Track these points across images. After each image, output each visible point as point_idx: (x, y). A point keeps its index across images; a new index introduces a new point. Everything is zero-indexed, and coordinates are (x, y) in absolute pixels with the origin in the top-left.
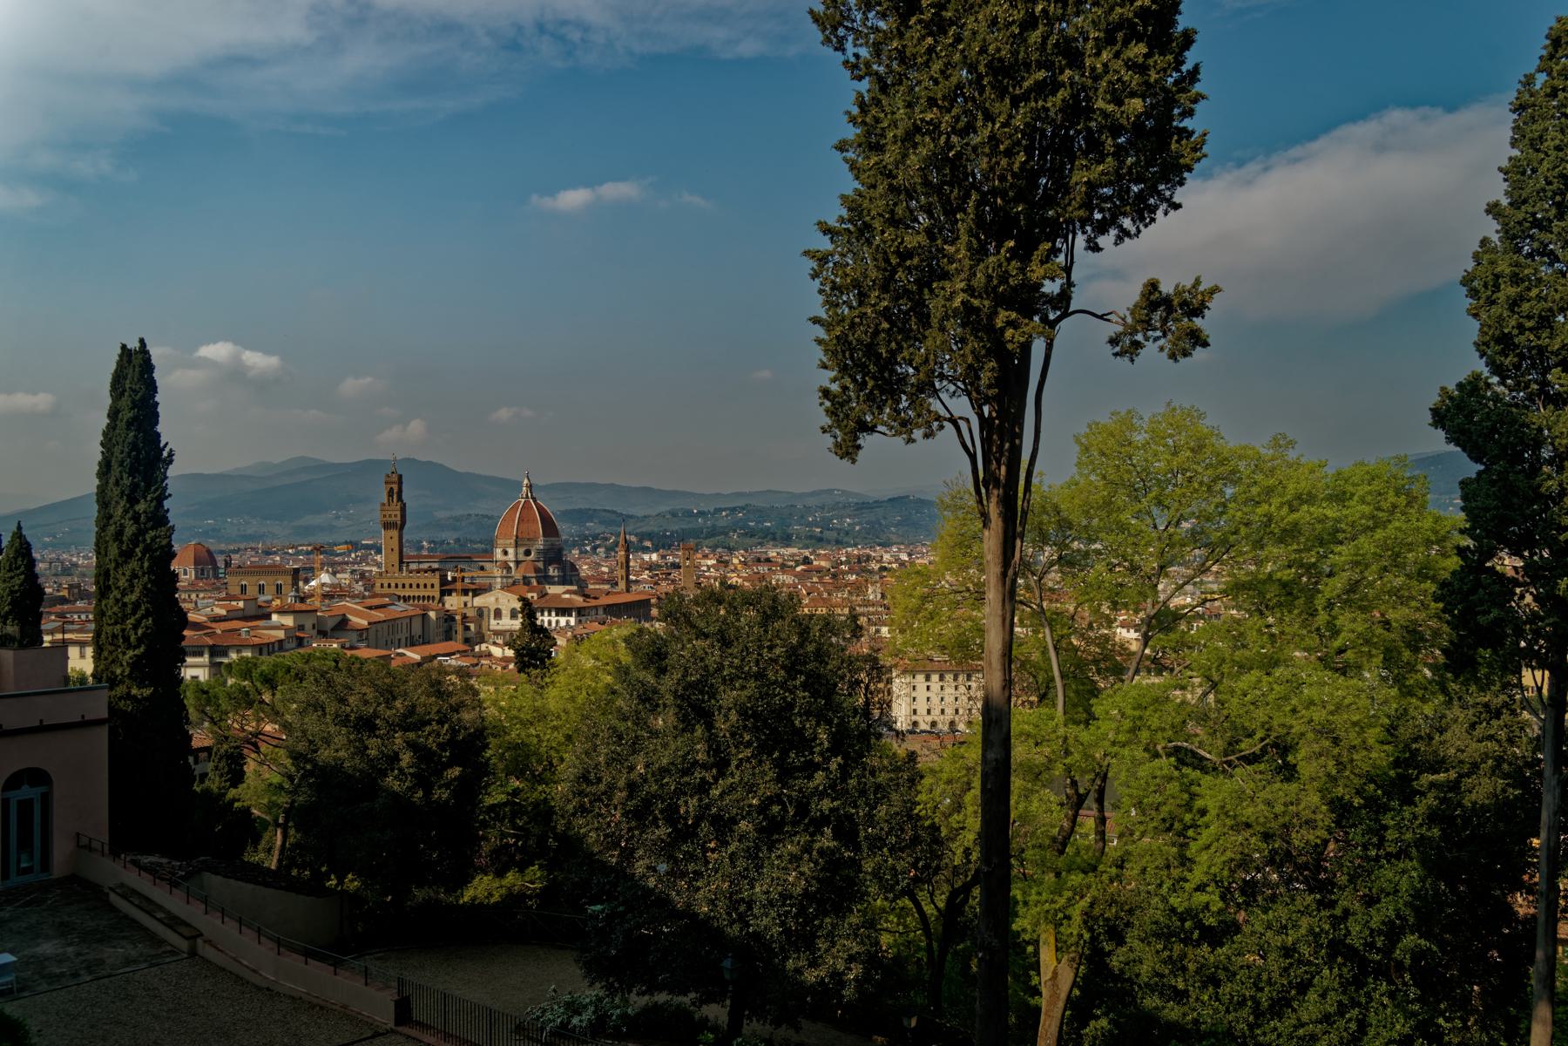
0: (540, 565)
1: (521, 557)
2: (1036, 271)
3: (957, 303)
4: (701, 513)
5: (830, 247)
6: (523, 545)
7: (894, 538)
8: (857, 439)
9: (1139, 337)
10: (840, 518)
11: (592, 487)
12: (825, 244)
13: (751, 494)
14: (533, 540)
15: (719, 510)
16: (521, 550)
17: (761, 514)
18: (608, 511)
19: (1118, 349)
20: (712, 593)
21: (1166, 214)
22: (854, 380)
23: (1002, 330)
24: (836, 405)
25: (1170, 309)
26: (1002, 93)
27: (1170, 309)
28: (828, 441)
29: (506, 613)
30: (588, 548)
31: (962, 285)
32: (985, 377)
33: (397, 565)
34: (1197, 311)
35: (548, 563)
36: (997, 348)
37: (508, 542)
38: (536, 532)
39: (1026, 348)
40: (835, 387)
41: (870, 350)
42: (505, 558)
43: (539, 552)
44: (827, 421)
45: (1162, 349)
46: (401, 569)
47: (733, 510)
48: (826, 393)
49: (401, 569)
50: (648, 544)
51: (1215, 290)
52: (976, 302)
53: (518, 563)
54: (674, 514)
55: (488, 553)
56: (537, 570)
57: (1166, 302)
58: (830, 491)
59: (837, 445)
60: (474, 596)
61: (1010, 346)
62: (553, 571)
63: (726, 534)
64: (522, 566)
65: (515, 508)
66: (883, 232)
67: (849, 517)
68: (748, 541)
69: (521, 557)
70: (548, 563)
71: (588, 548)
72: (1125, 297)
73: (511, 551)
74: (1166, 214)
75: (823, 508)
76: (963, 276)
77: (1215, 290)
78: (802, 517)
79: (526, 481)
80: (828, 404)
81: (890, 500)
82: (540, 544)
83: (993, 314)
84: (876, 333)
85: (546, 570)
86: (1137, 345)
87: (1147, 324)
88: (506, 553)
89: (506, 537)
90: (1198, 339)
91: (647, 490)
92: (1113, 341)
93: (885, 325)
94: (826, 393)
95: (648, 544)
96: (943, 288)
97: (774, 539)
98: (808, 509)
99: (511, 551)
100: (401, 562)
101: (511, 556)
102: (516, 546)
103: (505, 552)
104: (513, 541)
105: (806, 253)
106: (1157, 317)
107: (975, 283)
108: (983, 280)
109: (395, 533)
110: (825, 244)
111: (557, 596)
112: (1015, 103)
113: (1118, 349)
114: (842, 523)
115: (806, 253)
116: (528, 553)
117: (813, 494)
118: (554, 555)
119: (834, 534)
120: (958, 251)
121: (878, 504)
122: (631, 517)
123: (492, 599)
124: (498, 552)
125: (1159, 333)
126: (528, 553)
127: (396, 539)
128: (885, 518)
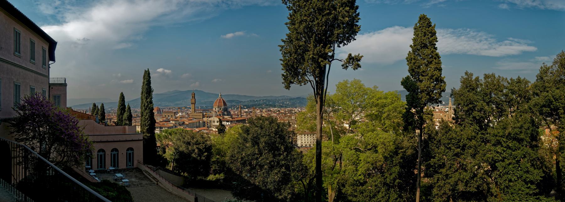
0: (223, 112)
1: (219, 110)
2: (327, 50)
3: (311, 56)
4: (257, 101)
5: (284, 45)
7: (297, 106)
8: (290, 85)
9: (348, 65)
10: (286, 102)
11: (234, 95)
12: (283, 44)
13: (267, 97)
14: (222, 106)
15: (260, 100)
16: (219, 109)
17: (269, 101)
19: (343, 67)
20: (259, 118)
21: (353, 41)
22: (289, 73)
23: (320, 62)
24: (285, 78)
25: (354, 60)
26: (320, 14)
27: (354, 60)
28: (284, 85)
29: (216, 121)
30: (233, 108)
31: (312, 53)
32: (317, 72)
34: (359, 60)
35: (224, 111)
36: (319, 66)
38: (222, 105)
39: (325, 66)
40: (285, 74)
41: (293, 66)
42: (216, 110)
43: (223, 109)
44: (283, 81)
45: (352, 68)
46: (195, 112)
47: (263, 100)
48: (283, 75)
49: (195, 112)
50: (245, 107)
51: (362, 56)
52: (315, 57)
53: (218, 111)
54: (251, 101)
55: (212, 109)
56: (222, 113)
57: (353, 58)
59: (286, 86)
61: (322, 66)
62: (225, 113)
63: (262, 105)
64: (219, 112)
66: (295, 42)
69: (219, 110)
70: (224, 111)
72: (345, 57)
73: (217, 109)
74: (353, 41)
75: (282, 99)
76: (312, 51)
77: (362, 56)
78: (278, 102)
79: (220, 94)
80: (283, 77)
81: (297, 98)
82: (223, 107)
83: (318, 59)
84: (294, 62)
85: (224, 113)
86: (347, 66)
87: (349, 62)
88: (216, 109)
89: (216, 106)
90: (359, 66)
91: (245, 96)
92: (343, 66)
93: (296, 61)
94: (283, 75)
95: (245, 107)
96: (308, 53)
97: (272, 106)
98: (279, 100)
99: (217, 109)
100: (195, 111)
101: (217, 110)
103: (216, 109)
104: (217, 107)
105: (279, 46)
106: (351, 61)
107: (314, 52)
108: (316, 52)
109: (194, 105)
110: (283, 44)
111: (227, 118)
112: (323, 16)
113: (343, 67)
114: (286, 103)
115: (279, 46)
116: (220, 109)
117: (280, 97)
118: (226, 110)
119: (285, 105)
120: (311, 46)
122: (241, 101)
124: (214, 109)
125: (351, 64)
126: (220, 109)
127: (194, 107)
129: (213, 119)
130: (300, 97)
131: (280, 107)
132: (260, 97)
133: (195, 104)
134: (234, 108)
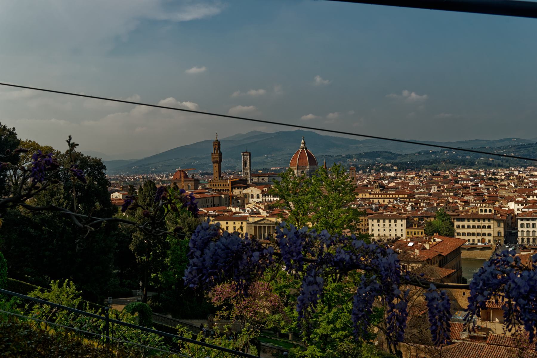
6: (300, 169)
13: (466, 142)
14: (305, 166)
16: (300, 171)
18: (386, 152)
30: (367, 170)
33: (218, 177)
37: (295, 167)
43: (307, 172)
46: (219, 179)
49: (219, 179)
50: (396, 168)
54: (419, 153)
58: (510, 139)
60: (243, 189)
63: (439, 162)
68: (449, 166)
71: (367, 170)
75: (500, 148)
95: (396, 168)
97: (464, 164)
102: (298, 169)
104: (296, 167)
117: (501, 141)
122: (399, 155)
126: (302, 172)
127: (217, 168)
128: (533, 153)
129: (250, 190)
131: (485, 165)
133: (220, 161)
134: (370, 170)
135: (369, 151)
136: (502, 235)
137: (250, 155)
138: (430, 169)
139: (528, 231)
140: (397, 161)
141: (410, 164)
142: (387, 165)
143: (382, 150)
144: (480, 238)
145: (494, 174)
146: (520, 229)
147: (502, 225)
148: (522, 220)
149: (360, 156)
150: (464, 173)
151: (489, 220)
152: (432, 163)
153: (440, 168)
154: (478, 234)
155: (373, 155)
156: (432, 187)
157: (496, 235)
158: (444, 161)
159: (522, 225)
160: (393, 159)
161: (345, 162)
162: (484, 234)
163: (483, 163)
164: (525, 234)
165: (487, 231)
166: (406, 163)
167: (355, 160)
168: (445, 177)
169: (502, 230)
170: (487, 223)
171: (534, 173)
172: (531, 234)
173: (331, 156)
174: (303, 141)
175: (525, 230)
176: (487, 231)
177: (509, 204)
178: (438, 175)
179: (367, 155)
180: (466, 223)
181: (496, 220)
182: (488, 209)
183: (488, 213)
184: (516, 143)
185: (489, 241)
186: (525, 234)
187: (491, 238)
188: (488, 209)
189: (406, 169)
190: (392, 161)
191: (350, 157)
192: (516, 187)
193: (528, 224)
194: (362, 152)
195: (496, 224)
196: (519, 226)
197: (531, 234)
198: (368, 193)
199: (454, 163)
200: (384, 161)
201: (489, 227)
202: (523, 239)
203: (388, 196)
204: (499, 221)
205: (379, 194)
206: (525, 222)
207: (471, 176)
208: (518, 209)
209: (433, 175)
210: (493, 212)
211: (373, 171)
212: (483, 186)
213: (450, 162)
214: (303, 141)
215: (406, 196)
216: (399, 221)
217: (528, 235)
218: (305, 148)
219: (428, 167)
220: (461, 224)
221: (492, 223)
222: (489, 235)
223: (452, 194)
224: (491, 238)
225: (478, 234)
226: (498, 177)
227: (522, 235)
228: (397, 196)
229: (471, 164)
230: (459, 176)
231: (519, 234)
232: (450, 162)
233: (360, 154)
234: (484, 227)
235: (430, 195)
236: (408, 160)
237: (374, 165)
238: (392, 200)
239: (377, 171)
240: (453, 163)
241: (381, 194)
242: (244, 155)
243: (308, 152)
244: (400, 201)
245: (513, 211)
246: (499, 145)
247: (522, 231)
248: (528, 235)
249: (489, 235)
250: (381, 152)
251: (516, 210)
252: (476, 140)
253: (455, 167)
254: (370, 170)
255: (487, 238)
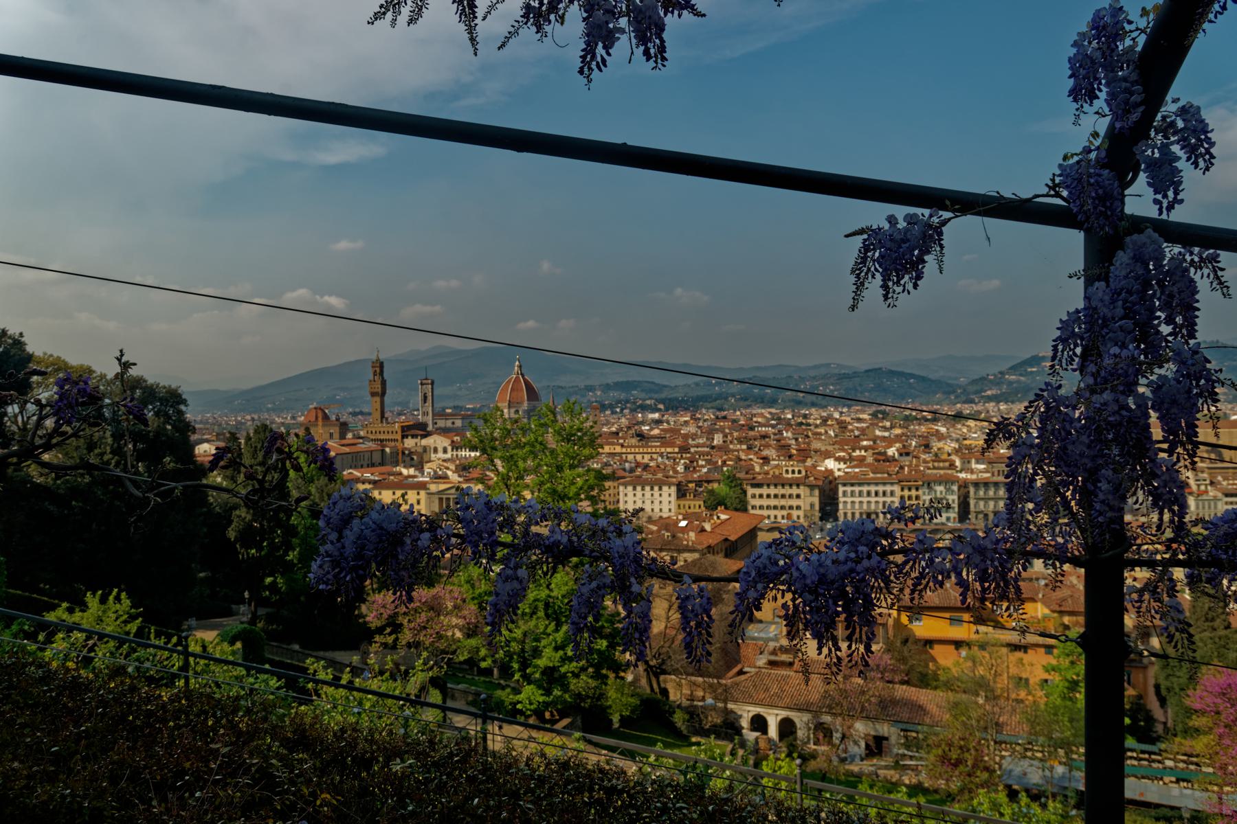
10: (826, 385)
16: (513, 410)
30: (618, 410)
43: (524, 411)
50: (661, 406)
63: (726, 399)
65: (509, 381)
67: (832, 384)
68: (742, 403)
71: (618, 410)
75: (814, 378)
81: (867, 371)
82: (525, 405)
95: (661, 406)
97: (762, 402)
102: (510, 407)
114: (825, 389)
117: (815, 367)
121: (856, 374)
122: (665, 386)
123: (432, 441)
126: (517, 412)
128: (860, 385)
130: (880, 369)
132: (741, 369)
134: (622, 410)
135: (621, 379)
136: (817, 507)
137: (432, 383)
138: (712, 408)
139: (853, 502)
140: (663, 396)
141: (683, 400)
142: (648, 402)
143: (641, 379)
144: (785, 513)
145: (805, 416)
146: (842, 499)
147: (817, 492)
148: (844, 485)
149: (607, 387)
150: (762, 415)
151: (798, 486)
152: (715, 400)
153: (726, 406)
154: (783, 508)
155: (627, 386)
156: (716, 436)
157: (808, 508)
158: (733, 396)
159: (845, 493)
160: (656, 392)
161: (583, 396)
162: (791, 508)
163: (790, 401)
164: (849, 506)
165: (794, 502)
166: (676, 399)
167: (599, 393)
168: (734, 421)
169: (816, 500)
170: (795, 491)
171: (861, 416)
172: (857, 506)
173: (562, 387)
174: (517, 363)
175: (849, 500)
176: (794, 502)
177: (827, 461)
178: (725, 418)
179: (618, 386)
180: (765, 491)
181: (808, 486)
182: (796, 469)
183: (796, 475)
184: (836, 371)
185: (798, 517)
186: (849, 506)
187: (801, 513)
188: (796, 469)
189: (677, 408)
190: (656, 396)
191: (591, 388)
192: (836, 436)
193: (852, 492)
194: (610, 381)
195: (807, 490)
196: (840, 494)
197: (857, 506)
198: (618, 444)
199: (747, 400)
200: (643, 395)
201: (798, 496)
202: (845, 514)
203: (649, 450)
204: (812, 487)
205: (635, 447)
206: (849, 489)
207: (773, 419)
208: (839, 470)
209: (717, 418)
210: (803, 473)
211: (626, 411)
212: (790, 434)
213: (742, 399)
214: (517, 363)
215: (677, 450)
216: (665, 488)
217: (853, 507)
218: (522, 374)
219: (709, 405)
220: (757, 491)
221: (802, 491)
222: (798, 508)
223: (744, 447)
224: (801, 513)
225: (783, 508)
226: (811, 421)
227: (845, 507)
228: (663, 450)
229: (772, 402)
230: (755, 419)
231: (841, 506)
232: (742, 399)
233: (608, 384)
234: (791, 496)
235: (713, 447)
236: (679, 395)
237: (627, 401)
238: (655, 456)
239: (633, 411)
240: (746, 399)
241: (639, 447)
242: (422, 384)
243: (526, 382)
244: (668, 458)
245: (831, 472)
246: (812, 373)
247: (845, 502)
248: (853, 507)
249: (798, 508)
250: (639, 382)
251: (836, 470)
252: (780, 366)
253: (749, 406)
254: (622, 410)
255: (795, 513)
